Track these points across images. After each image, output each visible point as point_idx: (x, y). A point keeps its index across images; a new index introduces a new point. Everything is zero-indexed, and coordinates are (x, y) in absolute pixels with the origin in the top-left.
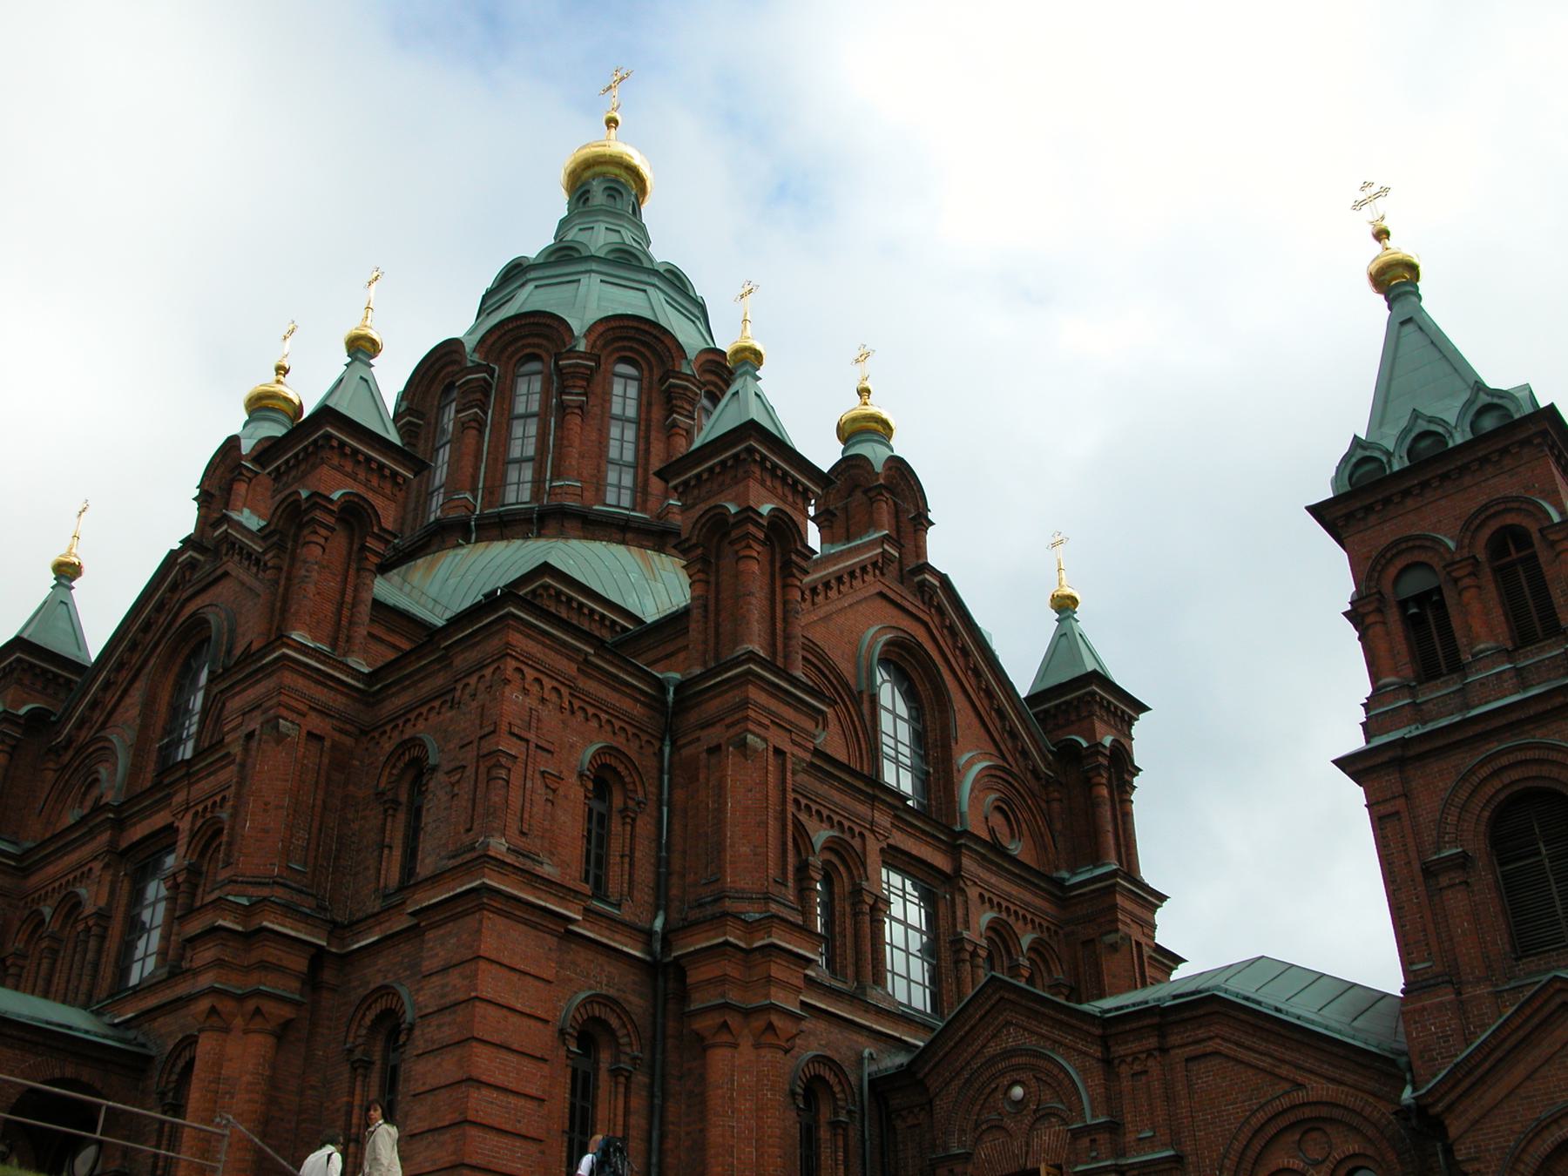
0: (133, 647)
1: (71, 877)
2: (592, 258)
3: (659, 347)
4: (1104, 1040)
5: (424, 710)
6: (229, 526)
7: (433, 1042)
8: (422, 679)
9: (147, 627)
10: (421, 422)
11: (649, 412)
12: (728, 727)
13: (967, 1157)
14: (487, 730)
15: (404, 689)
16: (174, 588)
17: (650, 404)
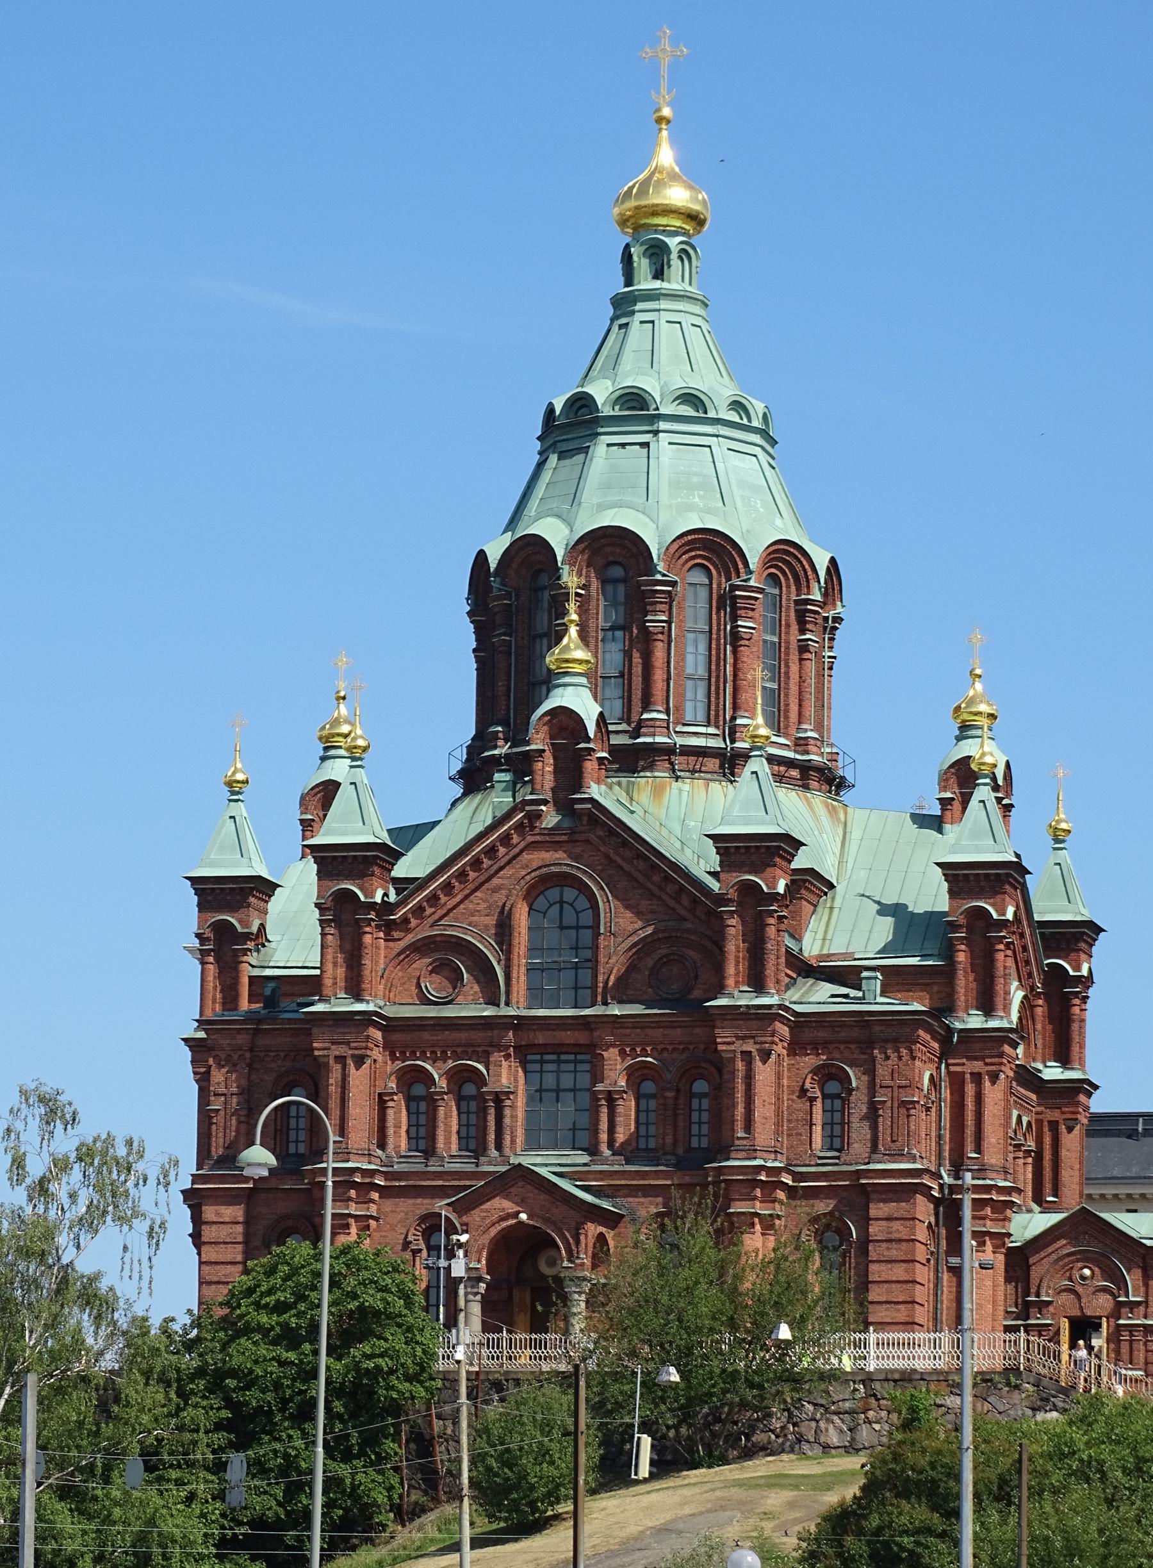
0: (476, 863)
1: (459, 1050)
2: (718, 421)
3: (798, 568)
4: (1144, 1258)
5: (842, 1047)
6: (593, 807)
7: (884, 1256)
8: (838, 1026)
9: (491, 851)
10: (583, 592)
11: (787, 633)
12: (986, 1064)
13: (1049, 1303)
14: (904, 1083)
15: (822, 1027)
16: (519, 827)
17: (788, 625)
